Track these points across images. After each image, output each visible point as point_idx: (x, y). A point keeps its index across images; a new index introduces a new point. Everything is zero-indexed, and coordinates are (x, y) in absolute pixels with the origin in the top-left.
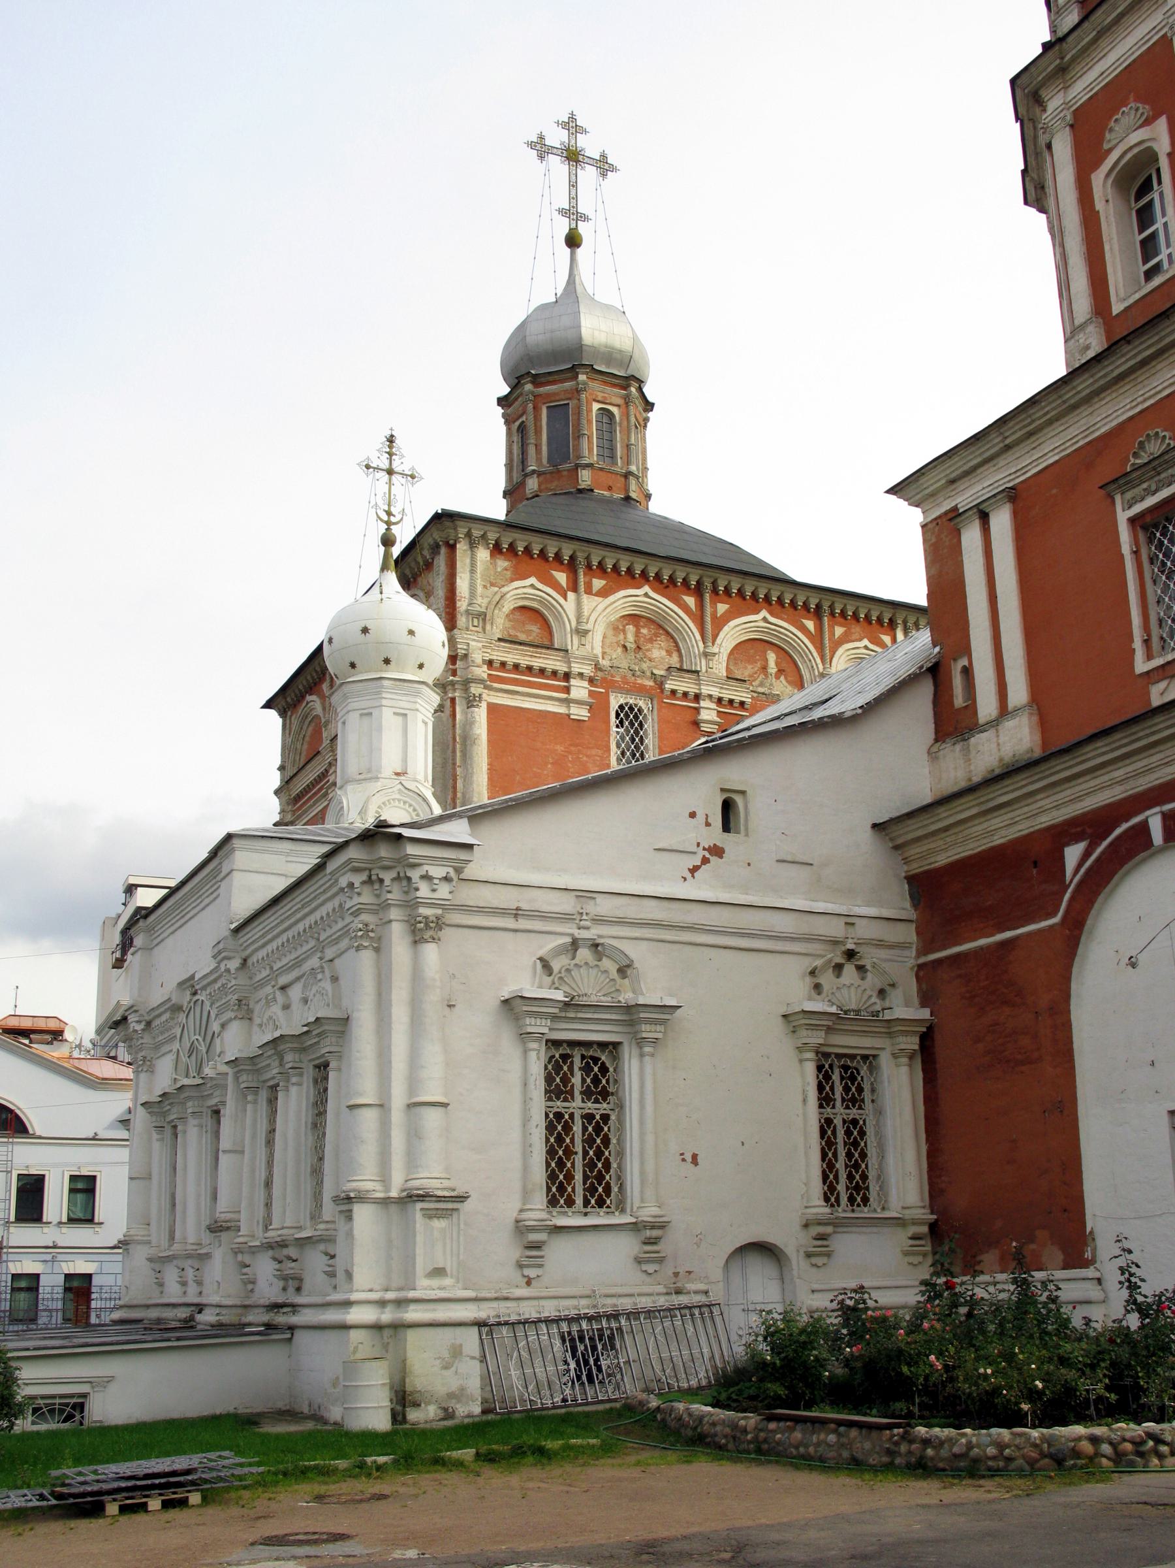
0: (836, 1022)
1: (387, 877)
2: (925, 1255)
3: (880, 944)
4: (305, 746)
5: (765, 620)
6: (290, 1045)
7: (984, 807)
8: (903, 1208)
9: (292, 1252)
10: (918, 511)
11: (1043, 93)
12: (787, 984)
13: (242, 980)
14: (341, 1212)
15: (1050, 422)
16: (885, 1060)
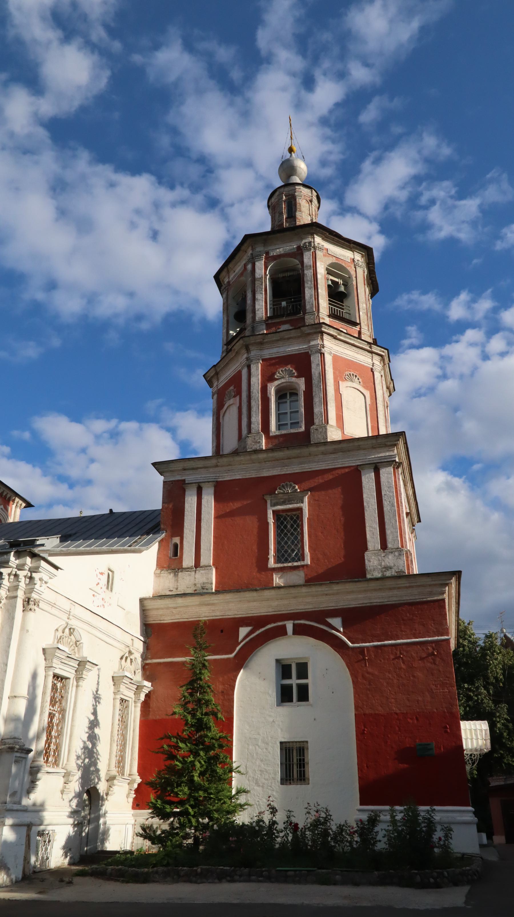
11: (251, 348)
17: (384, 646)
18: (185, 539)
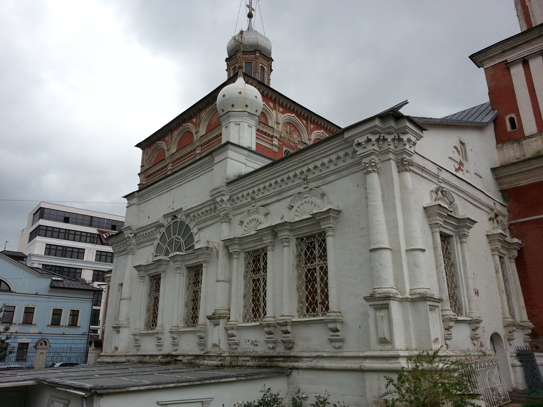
1: (390, 138)
4: (154, 159)
6: (287, 227)
9: (289, 328)
13: (228, 205)
14: (370, 305)
18: (521, 112)
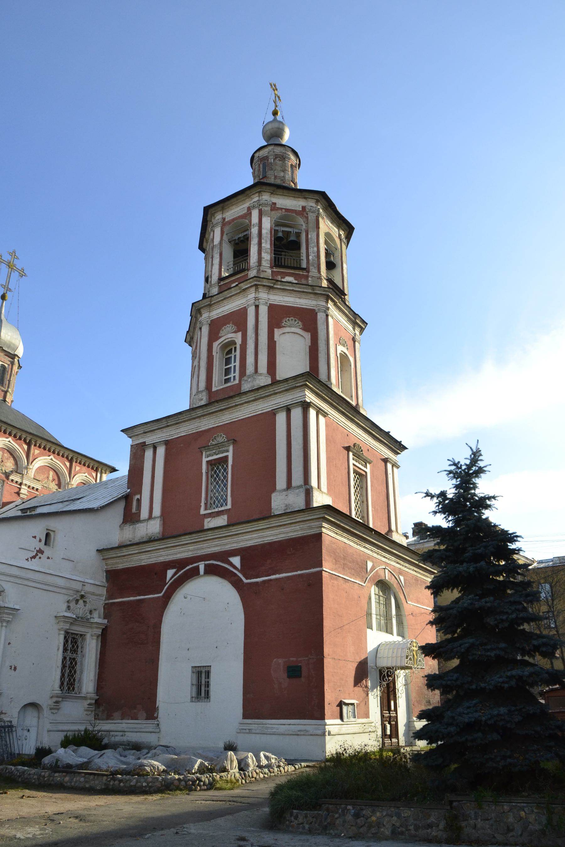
0: (75, 621)
2: (92, 711)
3: (93, 594)
5: (51, 459)
7: (140, 551)
8: (87, 693)
10: (130, 440)
11: (202, 310)
12: (58, 605)
15: (185, 421)
16: (88, 636)
17: (271, 580)
